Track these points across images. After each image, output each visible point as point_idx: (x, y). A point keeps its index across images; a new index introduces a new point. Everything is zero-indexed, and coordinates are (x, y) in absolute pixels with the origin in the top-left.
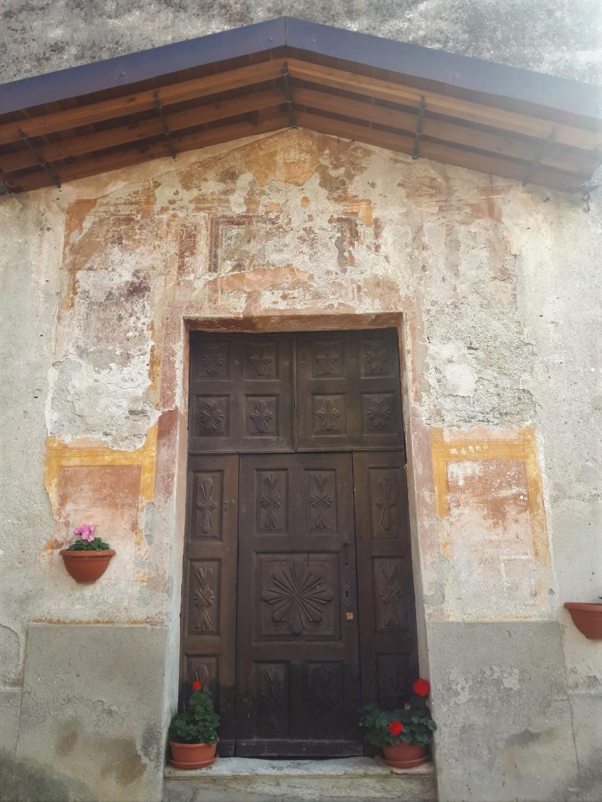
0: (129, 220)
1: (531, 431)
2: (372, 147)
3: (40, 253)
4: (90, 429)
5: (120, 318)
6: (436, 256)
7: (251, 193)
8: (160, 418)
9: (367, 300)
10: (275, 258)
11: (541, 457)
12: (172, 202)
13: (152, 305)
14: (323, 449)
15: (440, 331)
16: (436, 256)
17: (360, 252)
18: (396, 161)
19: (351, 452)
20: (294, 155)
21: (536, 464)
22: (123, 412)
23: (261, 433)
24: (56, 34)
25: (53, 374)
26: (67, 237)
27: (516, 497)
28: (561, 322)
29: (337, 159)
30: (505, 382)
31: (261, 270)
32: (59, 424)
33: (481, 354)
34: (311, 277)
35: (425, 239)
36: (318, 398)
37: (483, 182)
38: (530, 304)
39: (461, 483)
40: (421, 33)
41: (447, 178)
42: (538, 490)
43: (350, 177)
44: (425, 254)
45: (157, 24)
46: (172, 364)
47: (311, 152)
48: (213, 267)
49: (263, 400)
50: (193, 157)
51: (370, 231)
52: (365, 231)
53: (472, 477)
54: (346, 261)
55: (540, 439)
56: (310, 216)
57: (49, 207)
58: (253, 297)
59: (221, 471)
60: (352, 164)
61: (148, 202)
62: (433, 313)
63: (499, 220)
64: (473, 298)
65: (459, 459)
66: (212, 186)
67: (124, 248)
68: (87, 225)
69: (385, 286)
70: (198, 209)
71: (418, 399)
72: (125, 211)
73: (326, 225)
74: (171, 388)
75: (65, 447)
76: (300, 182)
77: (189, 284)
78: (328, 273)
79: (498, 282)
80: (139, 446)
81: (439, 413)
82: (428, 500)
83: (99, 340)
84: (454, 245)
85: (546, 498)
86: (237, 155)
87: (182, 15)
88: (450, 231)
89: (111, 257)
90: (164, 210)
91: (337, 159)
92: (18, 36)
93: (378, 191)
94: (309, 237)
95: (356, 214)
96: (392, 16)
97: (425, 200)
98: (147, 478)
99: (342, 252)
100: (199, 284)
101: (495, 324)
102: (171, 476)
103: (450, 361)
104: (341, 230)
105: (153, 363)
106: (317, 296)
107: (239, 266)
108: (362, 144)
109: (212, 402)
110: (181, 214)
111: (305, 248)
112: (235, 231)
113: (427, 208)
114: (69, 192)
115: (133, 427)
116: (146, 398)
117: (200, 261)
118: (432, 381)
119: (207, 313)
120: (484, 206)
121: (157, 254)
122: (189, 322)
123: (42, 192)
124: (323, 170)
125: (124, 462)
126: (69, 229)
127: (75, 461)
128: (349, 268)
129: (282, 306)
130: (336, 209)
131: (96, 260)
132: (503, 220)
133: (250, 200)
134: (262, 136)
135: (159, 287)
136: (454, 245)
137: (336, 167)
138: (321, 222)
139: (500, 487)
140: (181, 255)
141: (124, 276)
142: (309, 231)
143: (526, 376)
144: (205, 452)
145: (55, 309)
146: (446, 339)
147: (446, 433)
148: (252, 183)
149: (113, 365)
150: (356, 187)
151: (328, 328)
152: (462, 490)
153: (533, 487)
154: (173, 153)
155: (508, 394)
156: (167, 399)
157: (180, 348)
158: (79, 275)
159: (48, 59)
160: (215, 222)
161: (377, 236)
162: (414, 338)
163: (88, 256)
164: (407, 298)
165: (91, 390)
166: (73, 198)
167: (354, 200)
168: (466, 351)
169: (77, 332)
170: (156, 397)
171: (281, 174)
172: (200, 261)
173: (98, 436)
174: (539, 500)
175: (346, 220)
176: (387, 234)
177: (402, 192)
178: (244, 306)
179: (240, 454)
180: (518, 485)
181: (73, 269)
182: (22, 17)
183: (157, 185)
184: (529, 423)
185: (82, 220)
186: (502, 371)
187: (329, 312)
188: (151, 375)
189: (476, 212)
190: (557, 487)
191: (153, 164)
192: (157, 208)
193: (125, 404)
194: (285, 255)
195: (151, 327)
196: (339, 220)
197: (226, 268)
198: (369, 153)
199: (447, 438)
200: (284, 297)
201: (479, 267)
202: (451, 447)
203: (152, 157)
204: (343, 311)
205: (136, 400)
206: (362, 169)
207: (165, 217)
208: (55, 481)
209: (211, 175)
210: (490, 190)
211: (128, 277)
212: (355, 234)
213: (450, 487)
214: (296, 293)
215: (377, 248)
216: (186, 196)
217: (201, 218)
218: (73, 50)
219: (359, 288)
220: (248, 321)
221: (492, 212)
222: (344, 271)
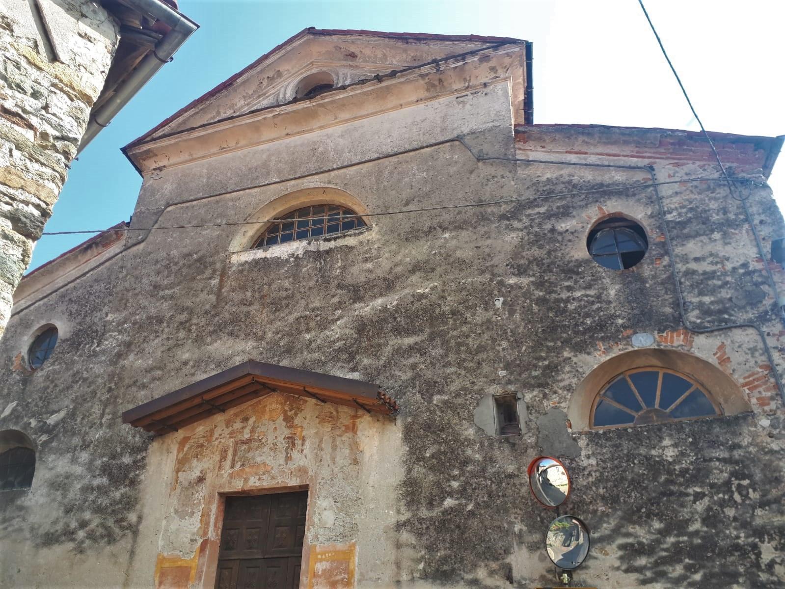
0: (202, 445)
1: (354, 545)
2: (308, 399)
3: (166, 465)
4: (174, 549)
5: (193, 494)
6: (326, 455)
7: (253, 427)
8: (202, 543)
9: (294, 479)
10: (258, 459)
11: (357, 558)
12: (220, 435)
13: (206, 487)
14: (275, 556)
15: (324, 493)
16: (326, 455)
17: (295, 454)
18: (317, 405)
19: (288, 557)
20: (274, 406)
21: (353, 562)
22: (187, 540)
23: (251, 548)
24: (186, 356)
25: (164, 522)
26: (177, 456)
27: (342, 580)
28: (376, 486)
29: (292, 406)
30: (348, 519)
31: (251, 466)
32: (163, 547)
33: (339, 505)
34: (272, 468)
35: (323, 445)
36: (278, 528)
37: (353, 413)
38: (364, 477)
39: (320, 573)
40: (337, 336)
41: (337, 412)
42: (353, 575)
43: (296, 414)
44: (322, 452)
45: (227, 346)
46: (209, 516)
47: (281, 404)
48: (232, 466)
49: (253, 531)
50: (232, 412)
51: (300, 442)
52: (298, 442)
53: (325, 570)
54: (288, 458)
55: (358, 549)
56: (276, 437)
57: (172, 442)
58: (246, 480)
59: (231, 568)
60: (298, 408)
61: (211, 436)
62: (322, 484)
63: (356, 433)
64: (340, 475)
65: (321, 560)
66: (238, 425)
67: (198, 460)
68: (186, 449)
69: (303, 471)
70: (230, 438)
71: (309, 530)
72: (201, 440)
73: (283, 441)
74: (208, 528)
75: (164, 558)
76: (274, 419)
77: (222, 475)
78: (280, 465)
79: (352, 466)
80: (192, 557)
81: (316, 537)
82: (305, 582)
83: (183, 505)
84: (334, 447)
85: (356, 580)
86: (250, 408)
87: (237, 340)
88: (334, 439)
89: (193, 465)
90: (217, 439)
91: (292, 406)
92: (171, 360)
93: (307, 421)
94: (274, 448)
95: (295, 434)
96: (325, 329)
97: (326, 424)
98: (193, 572)
99: (287, 454)
100: (226, 475)
101: (349, 488)
102: (202, 572)
103: (325, 509)
104: (288, 443)
105: (202, 516)
106: (273, 478)
107: (243, 465)
108: (303, 398)
109: (232, 532)
110: (223, 441)
111: (272, 454)
112: (244, 447)
113: (327, 428)
114: (181, 434)
115: (191, 547)
116: (197, 533)
117: (227, 464)
118: (316, 520)
119: (227, 490)
120: (351, 426)
121: (211, 462)
122: (221, 494)
123: (171, 434)
124: (285, 412)
125: (185, 565)
126: (179, 452)
127: (167, 565)
128: (289, 462)
129: (258, 484)
130: (287, 432)
131: (187, 466)
132: (358, 433)
133: (252, 431)
134: (261, 398)
135: (210, 477)
136: (334, 447)
137: (291, 410)
138: (281, 439)
139: (336, 575)
140: (221, 461)
141: (197, 473)
142: (275, 444)
143: (357, 516)
144: (227, 558)
145: (169, 491)
146: (325, 497)
147: (318, 547)
148: (254, 422)
149: (187, 517)
150: (297, 421)
151: (280, 492)
152: (320, 577)
153: (351, 574)
154: (223, 411)
155: (347, 526)
156: (205, 533)
157: (214, 508)
158: (180, 474)
159: (181, 369)
160: (236, 443)
161: (303, 445)
162: (311, 498)
163: (184, 465)
164: (312, 476)
165: (178, 530)
166: (182, 436)
167: (296, 427)
168: (333, 503)
169: (175, 502)
170: (201, 533)
171: (267, 416)
172: (227, 464)
173: (177, 553)
174: (352, 581)
175: (291, 437)
176: (307, 444)
177: (317, 420)
178: (242, 485)
179: (240, 559)
180: (344, 573)
181: (178, 471)
182: (174, 350)
183: (216, 426)
184: (353, 541)
185: (184, 446)
186: (347, 514)
187: (277, 486)
188: (201, 521)
189: (347, 428)
190: (362, 574)
191: (215, 416)
192: (214, 438)
193: (189, 536)
194: (263, 458)
195: (204, 498)
196: (288, 438)
197: (238, 466)
198: (306, 401)
199: (318, 550)
200: (259, 479)
201: (345, 459)
202: (319, 554)
203: (214, 414)
204: (283, 485)
205: (193, 534)
206: (302, 410)
207: (216, 443)
208: (158, 575)
209: (238, 420)
210: (355, 417)
211: (198, 474)
212: (294, 444)
213: (315, 575)
214: (264, 477)
215: (302, 451)
216: (227, 431)
217: (231, 442)
218: (191, 363)
219: (292, 472)
220: (243, 492)
221: (353, 429)
222: (287, 464)
